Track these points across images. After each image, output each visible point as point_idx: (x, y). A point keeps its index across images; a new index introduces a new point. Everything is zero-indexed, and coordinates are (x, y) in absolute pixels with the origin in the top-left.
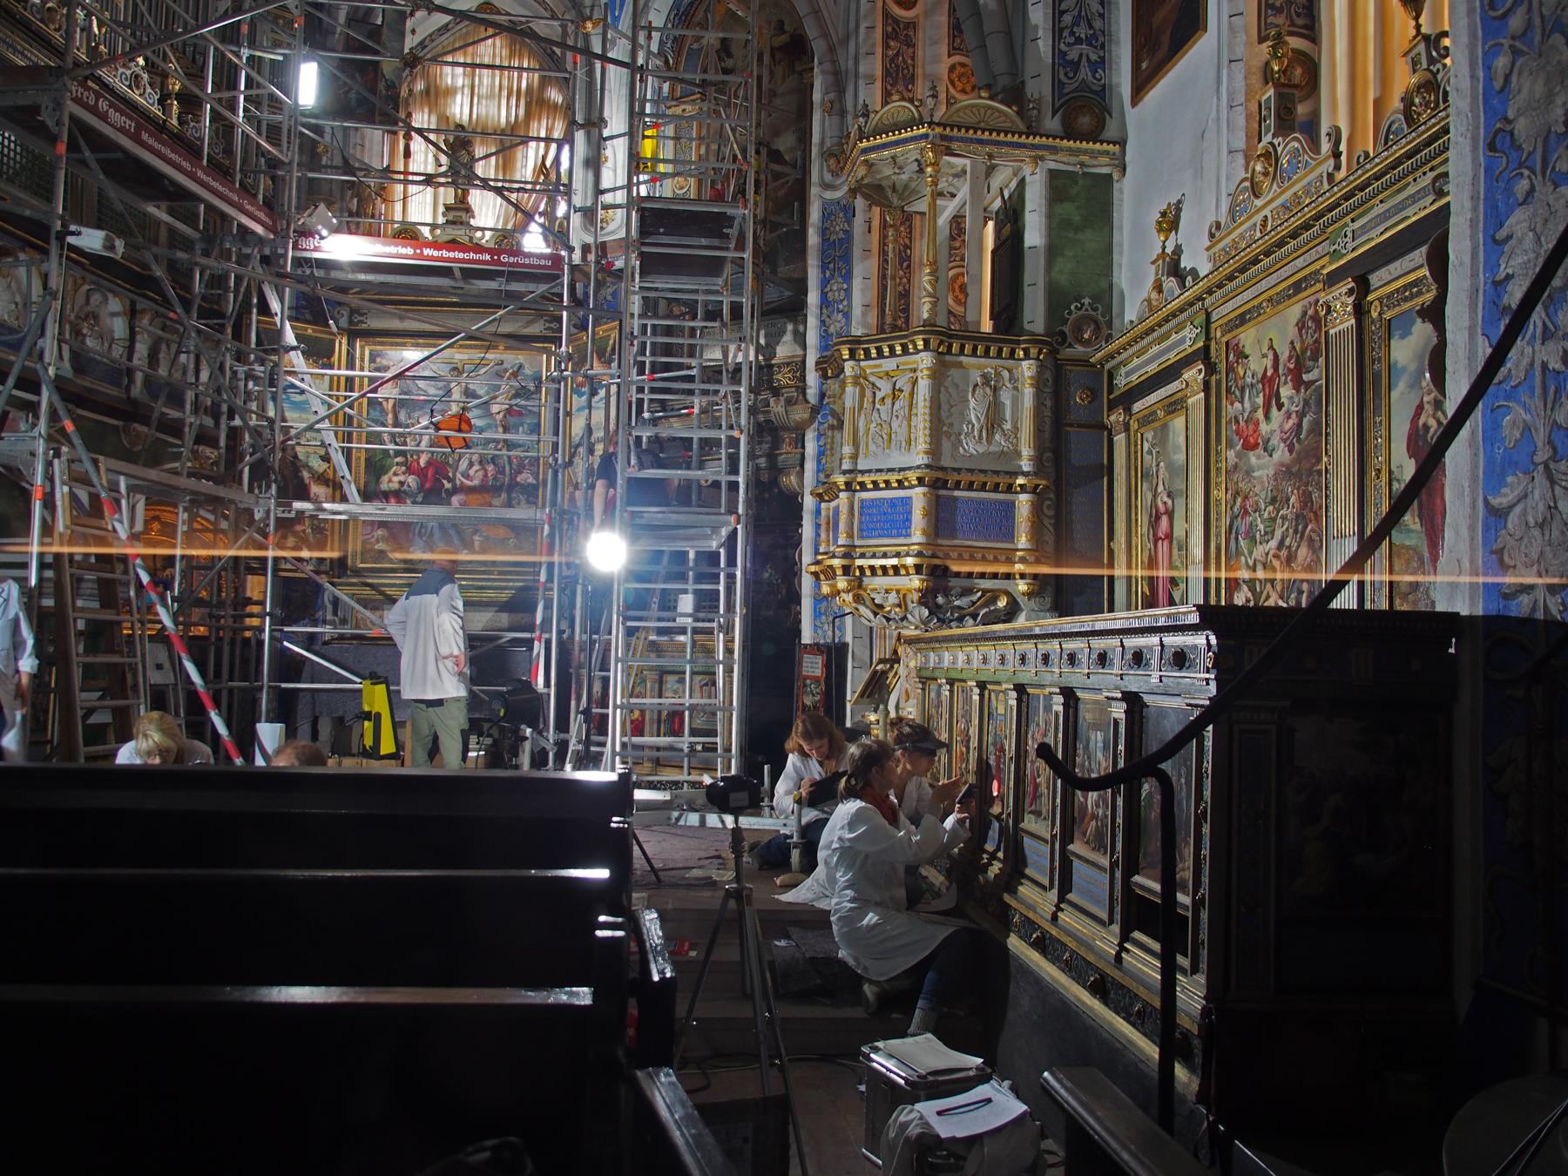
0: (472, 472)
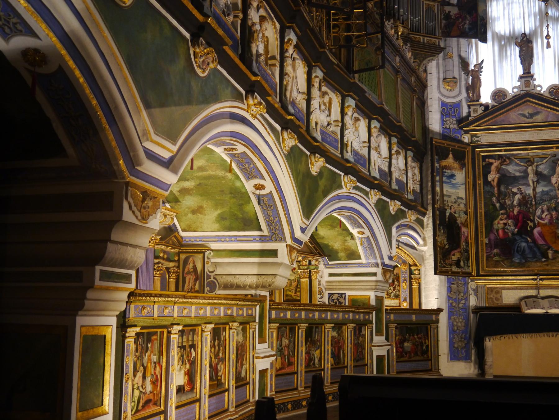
0: (543, 216)
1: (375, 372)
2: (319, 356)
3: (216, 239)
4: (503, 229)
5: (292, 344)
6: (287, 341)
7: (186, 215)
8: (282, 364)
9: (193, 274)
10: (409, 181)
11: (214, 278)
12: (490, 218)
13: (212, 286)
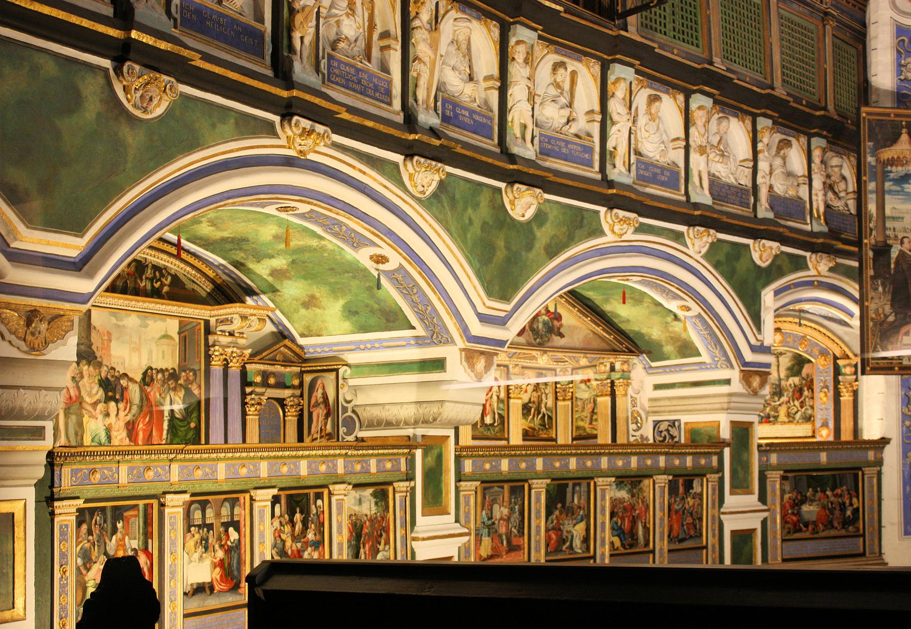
1: (728, 561)
2: (584, 533)
3: (353, 347)
5: (517, 514)
6: (505, 511)
7: (296, 311)
8: (493, 549)
9: (322, 406)
10: (814, 198)
11: (354, 411)
13: (350, 425)
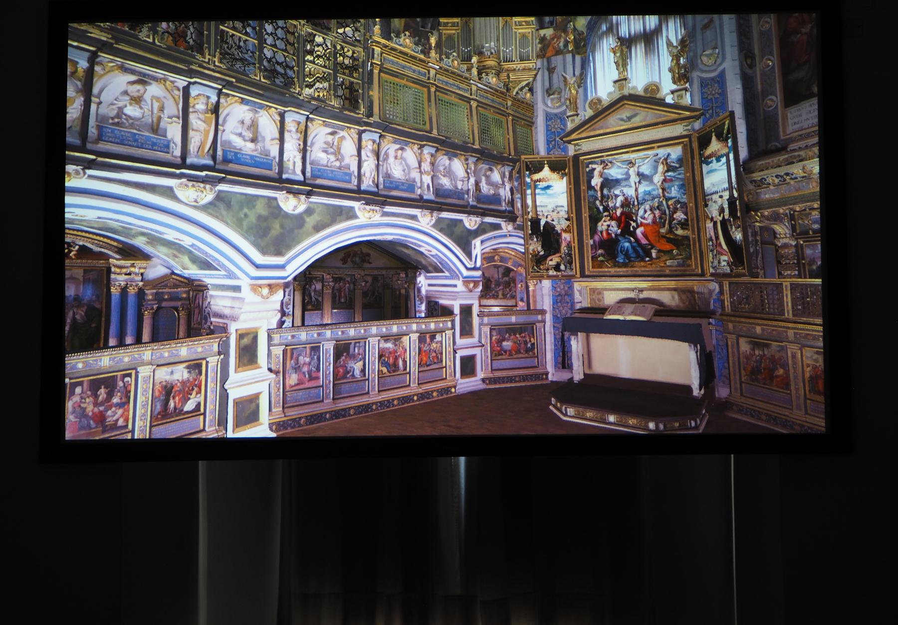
0: (646, 216)
4: (607, 230)
6: (307, 360)
12: (595, 219)
